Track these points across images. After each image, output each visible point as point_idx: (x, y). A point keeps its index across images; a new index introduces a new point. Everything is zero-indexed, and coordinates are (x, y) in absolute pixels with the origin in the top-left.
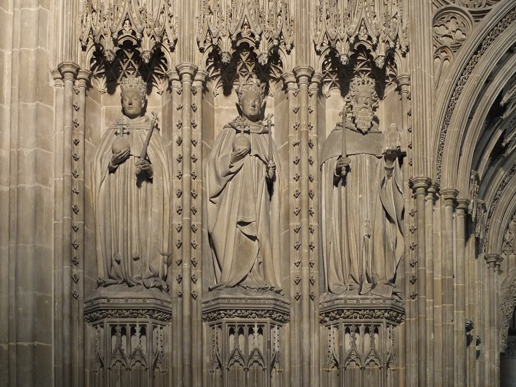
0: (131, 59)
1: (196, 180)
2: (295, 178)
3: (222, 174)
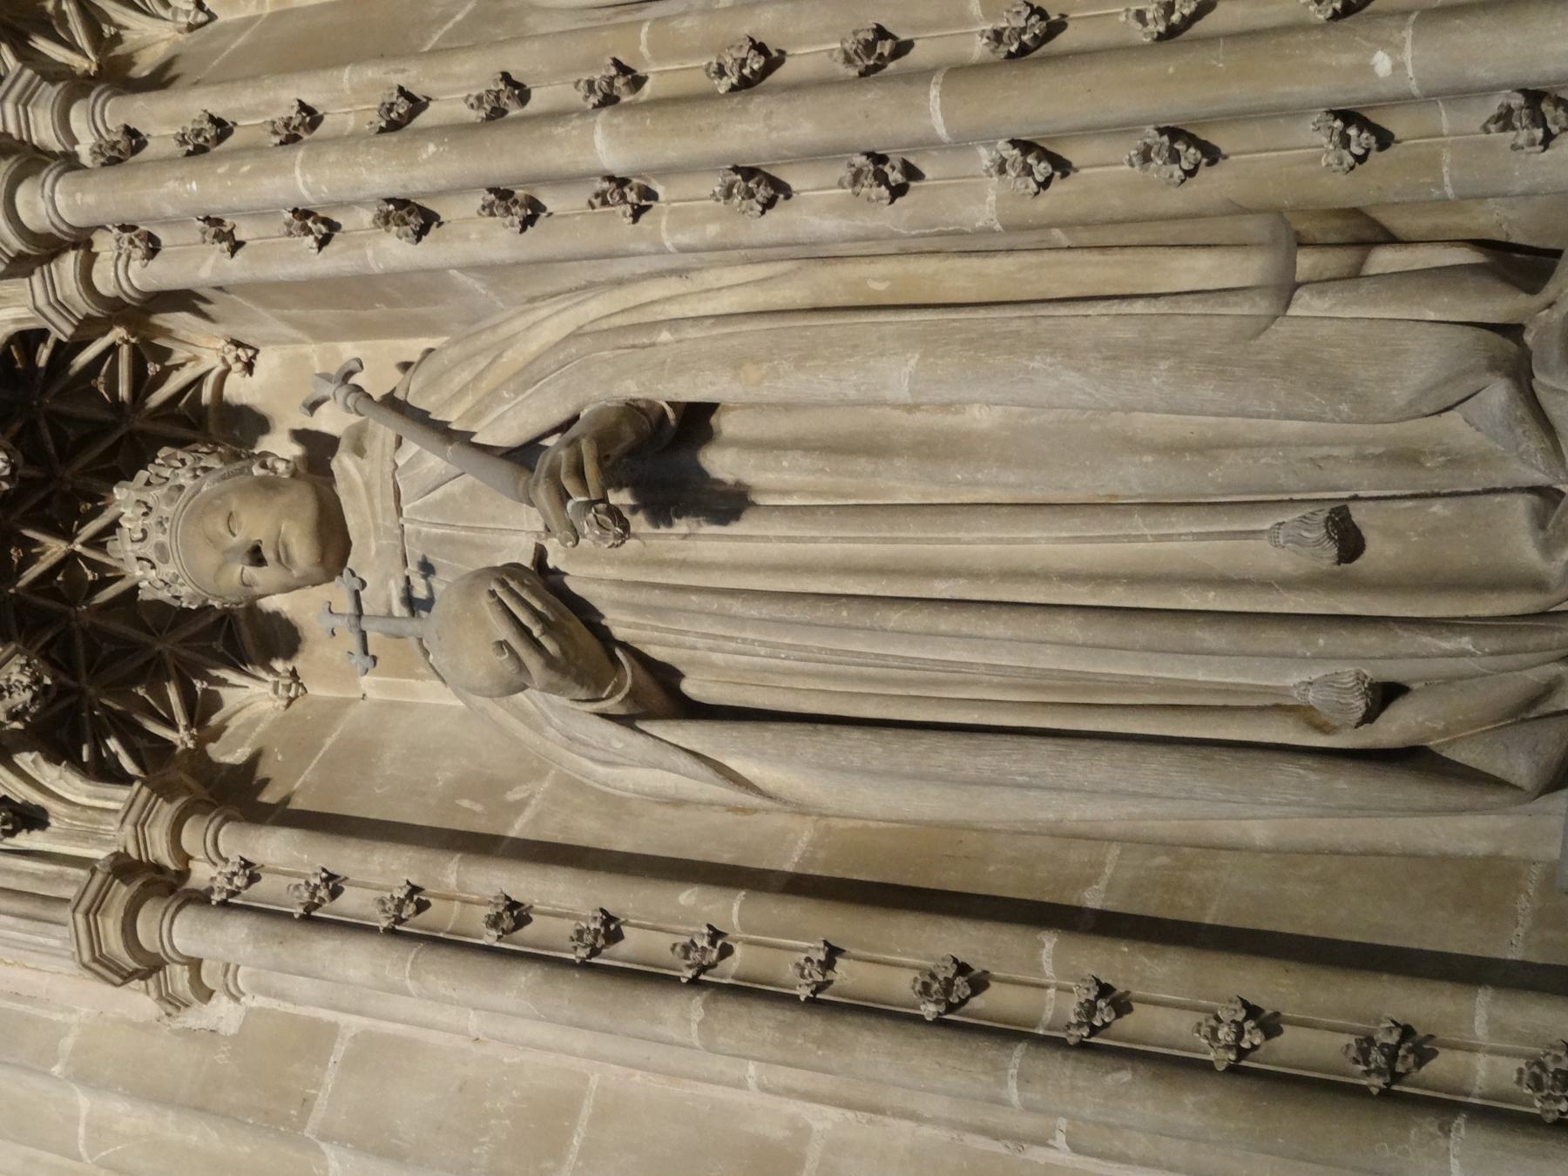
1: (648, 68)
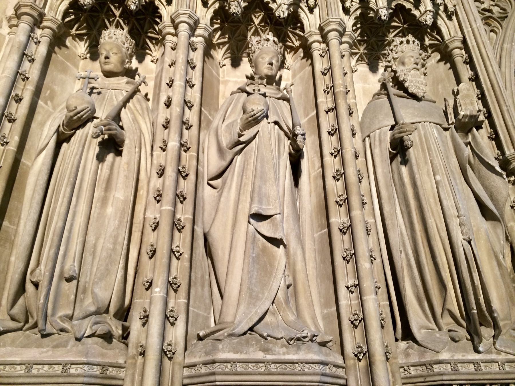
0: (120, 17)
2: (332, 154)
3: (227, 145)
